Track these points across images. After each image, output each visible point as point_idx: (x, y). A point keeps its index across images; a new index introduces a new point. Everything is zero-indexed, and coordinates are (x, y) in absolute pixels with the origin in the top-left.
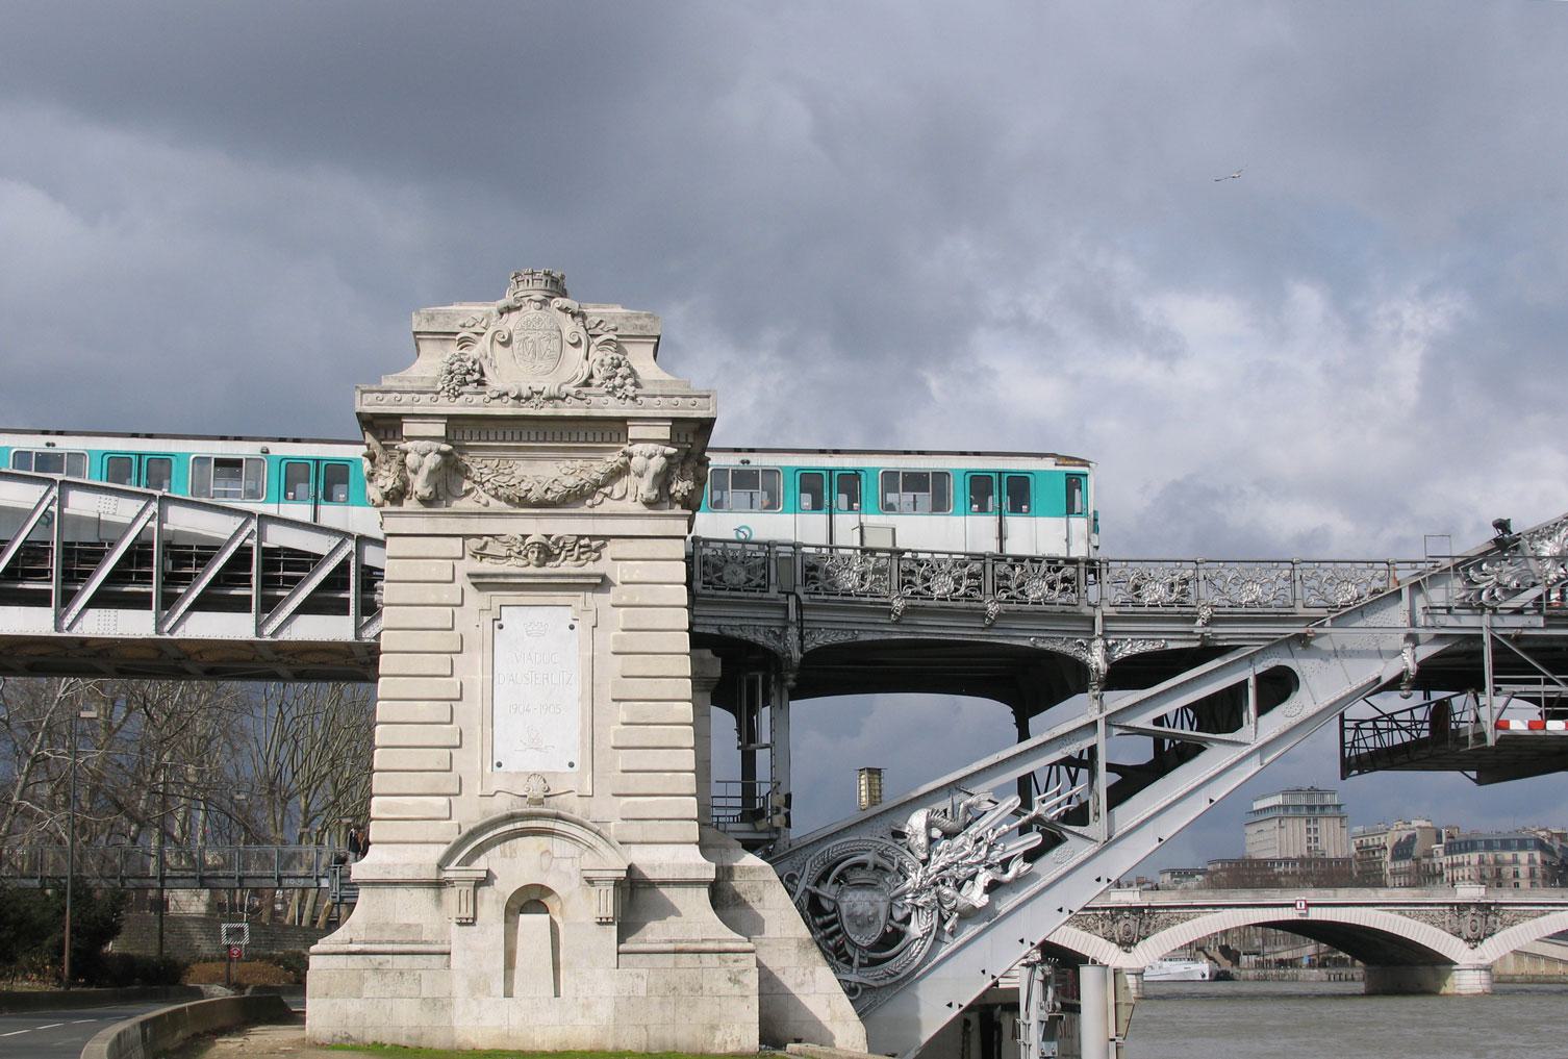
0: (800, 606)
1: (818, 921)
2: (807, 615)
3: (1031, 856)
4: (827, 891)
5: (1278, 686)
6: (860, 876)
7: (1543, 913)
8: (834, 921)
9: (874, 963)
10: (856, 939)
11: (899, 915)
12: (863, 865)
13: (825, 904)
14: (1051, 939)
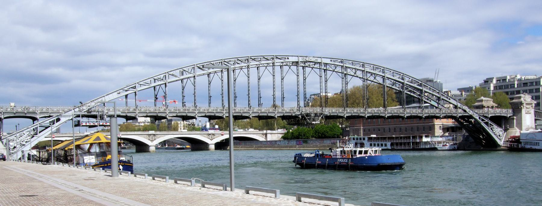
5: (58, 120)
6: (11, 141)
7: (165, 136)
9: (13, 150)
10: (11, 148)
14: (32, 147)
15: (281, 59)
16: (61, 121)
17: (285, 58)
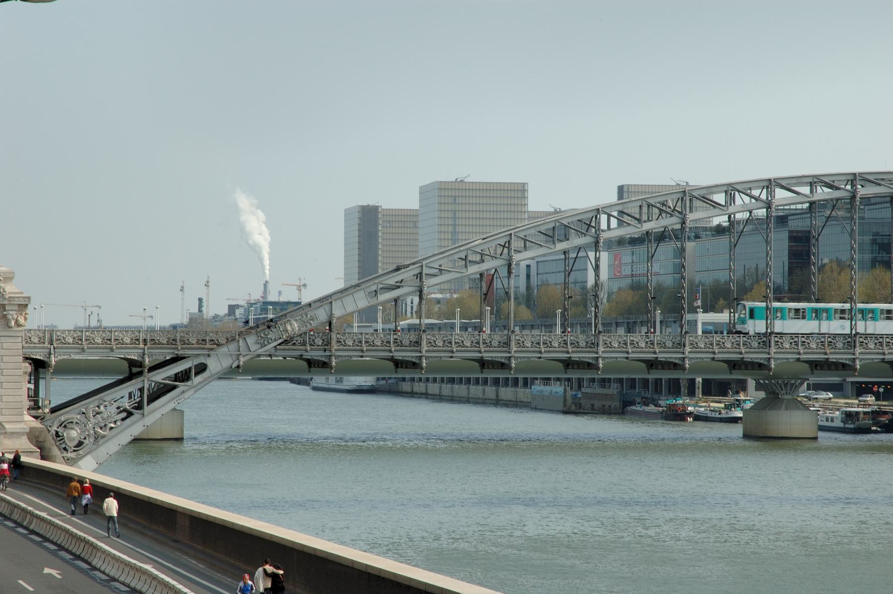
0: (54, 348)
1: (58, 439)
2: (56, 350)
3: (123, 419)
4: (60, 430)
6: (69, 426)
8: (63, 439)
9: (74, 451)
11: (82, 437)
12: (72, 422)
13: (60, 434)
15: (880, 185)
16: (208, 371)
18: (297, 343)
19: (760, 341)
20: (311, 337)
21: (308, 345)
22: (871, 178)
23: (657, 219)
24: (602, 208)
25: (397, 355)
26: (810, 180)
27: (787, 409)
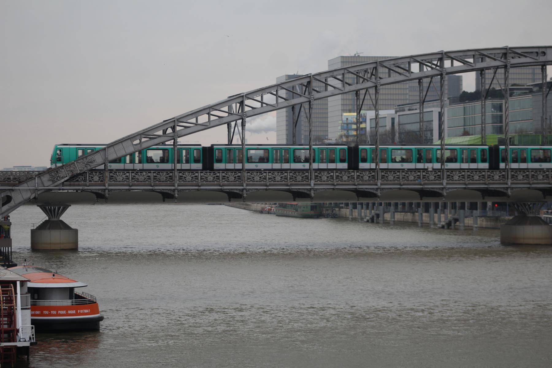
15: (526, 57)
17: (537, 53)
18: (79, 180)
19: (435, 175)
20: (90, 175)
21: (88, 181)
22: (519, 51)
23: (363, 82)
24: (313, 76)
25: (156, 188)
26: (473, 53)
27: (530, 224)
